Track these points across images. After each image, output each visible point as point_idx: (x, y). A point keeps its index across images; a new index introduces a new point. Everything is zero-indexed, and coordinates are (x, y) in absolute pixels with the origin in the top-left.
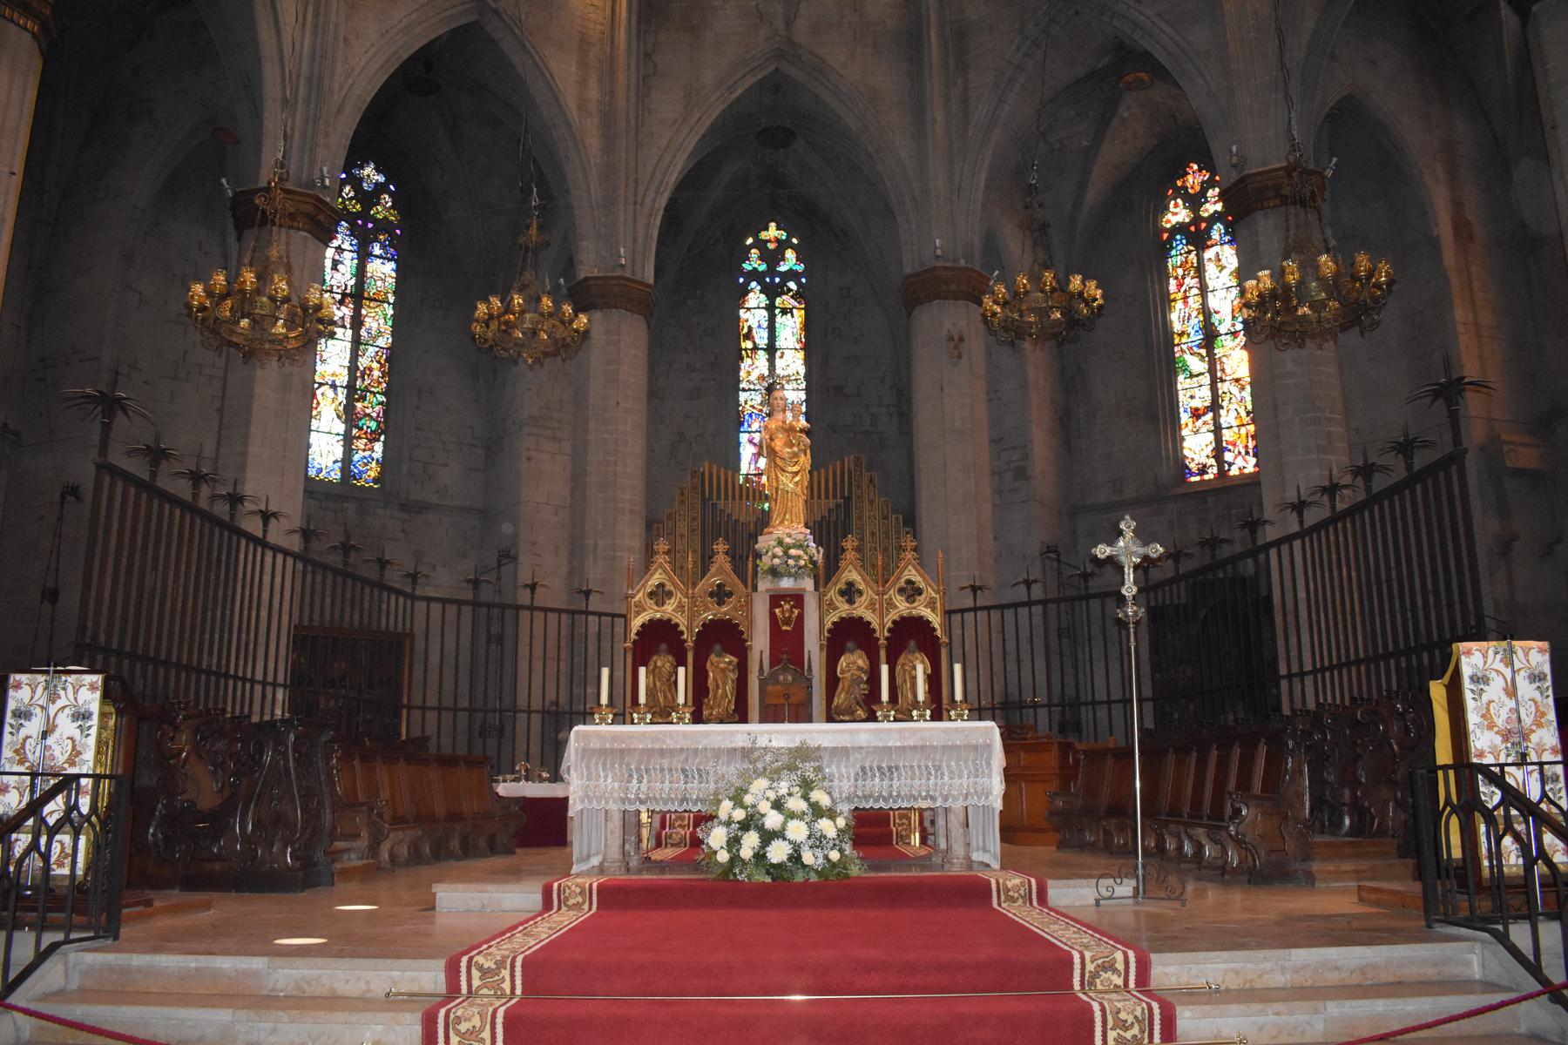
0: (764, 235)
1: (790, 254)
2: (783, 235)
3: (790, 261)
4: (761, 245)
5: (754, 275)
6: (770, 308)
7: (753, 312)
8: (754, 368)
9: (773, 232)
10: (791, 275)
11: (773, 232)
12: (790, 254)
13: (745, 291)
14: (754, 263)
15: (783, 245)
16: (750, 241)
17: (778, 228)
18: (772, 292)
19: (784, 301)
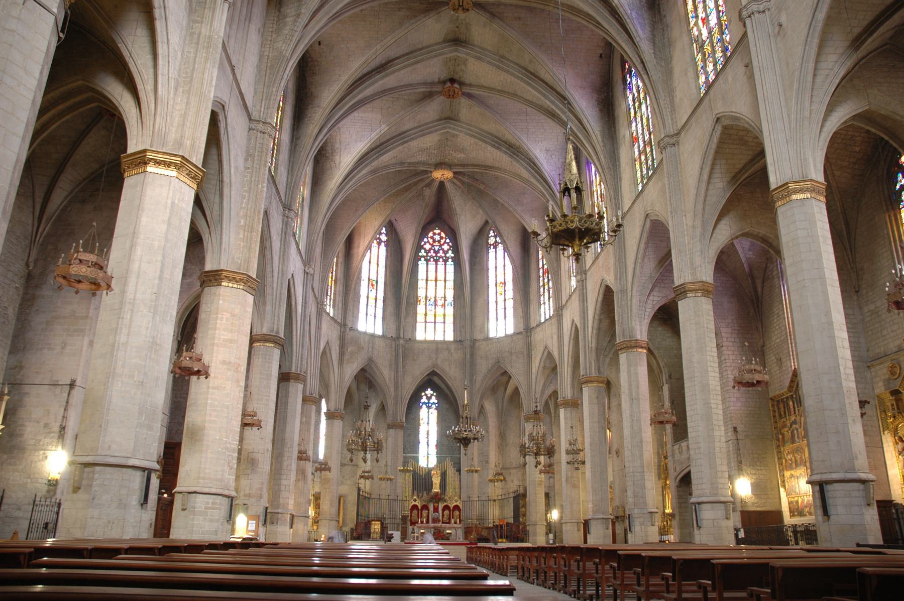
0: (427, 392)
1: (433, 398)
2: (432, 392)
3: (434, 400)
4: (426, 395)
5: (424, 403)
6: (428, 412)
7: (423, 412)
8: (423, 429)
9: (429, 392)
10: (434, 403)
11: (429, 392)
12: (433, 398)
13: (421, 407)
14: (424, 400)
15: (432, 395)
16: (423, 394)
17: (431, 390)
18: (429, 408)
19: (431, 410)
